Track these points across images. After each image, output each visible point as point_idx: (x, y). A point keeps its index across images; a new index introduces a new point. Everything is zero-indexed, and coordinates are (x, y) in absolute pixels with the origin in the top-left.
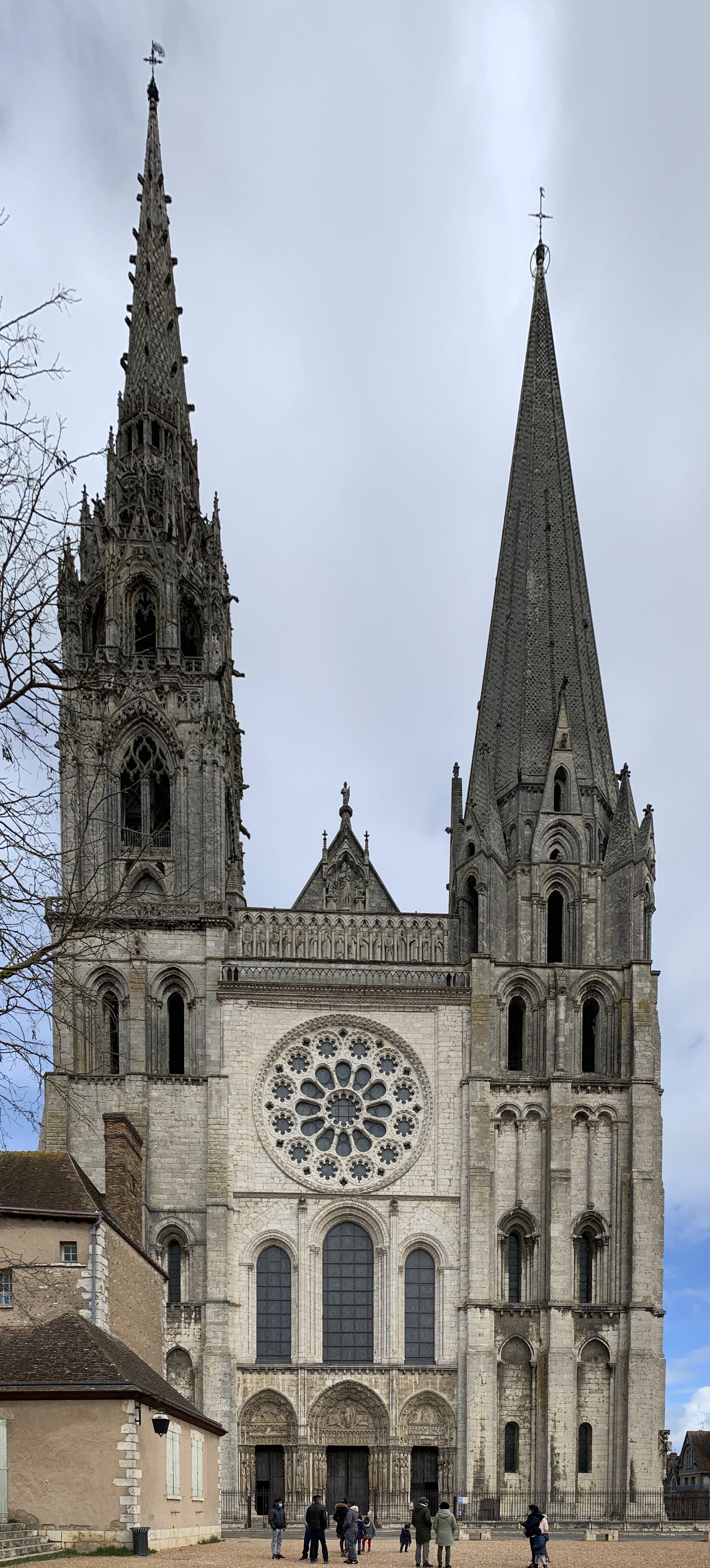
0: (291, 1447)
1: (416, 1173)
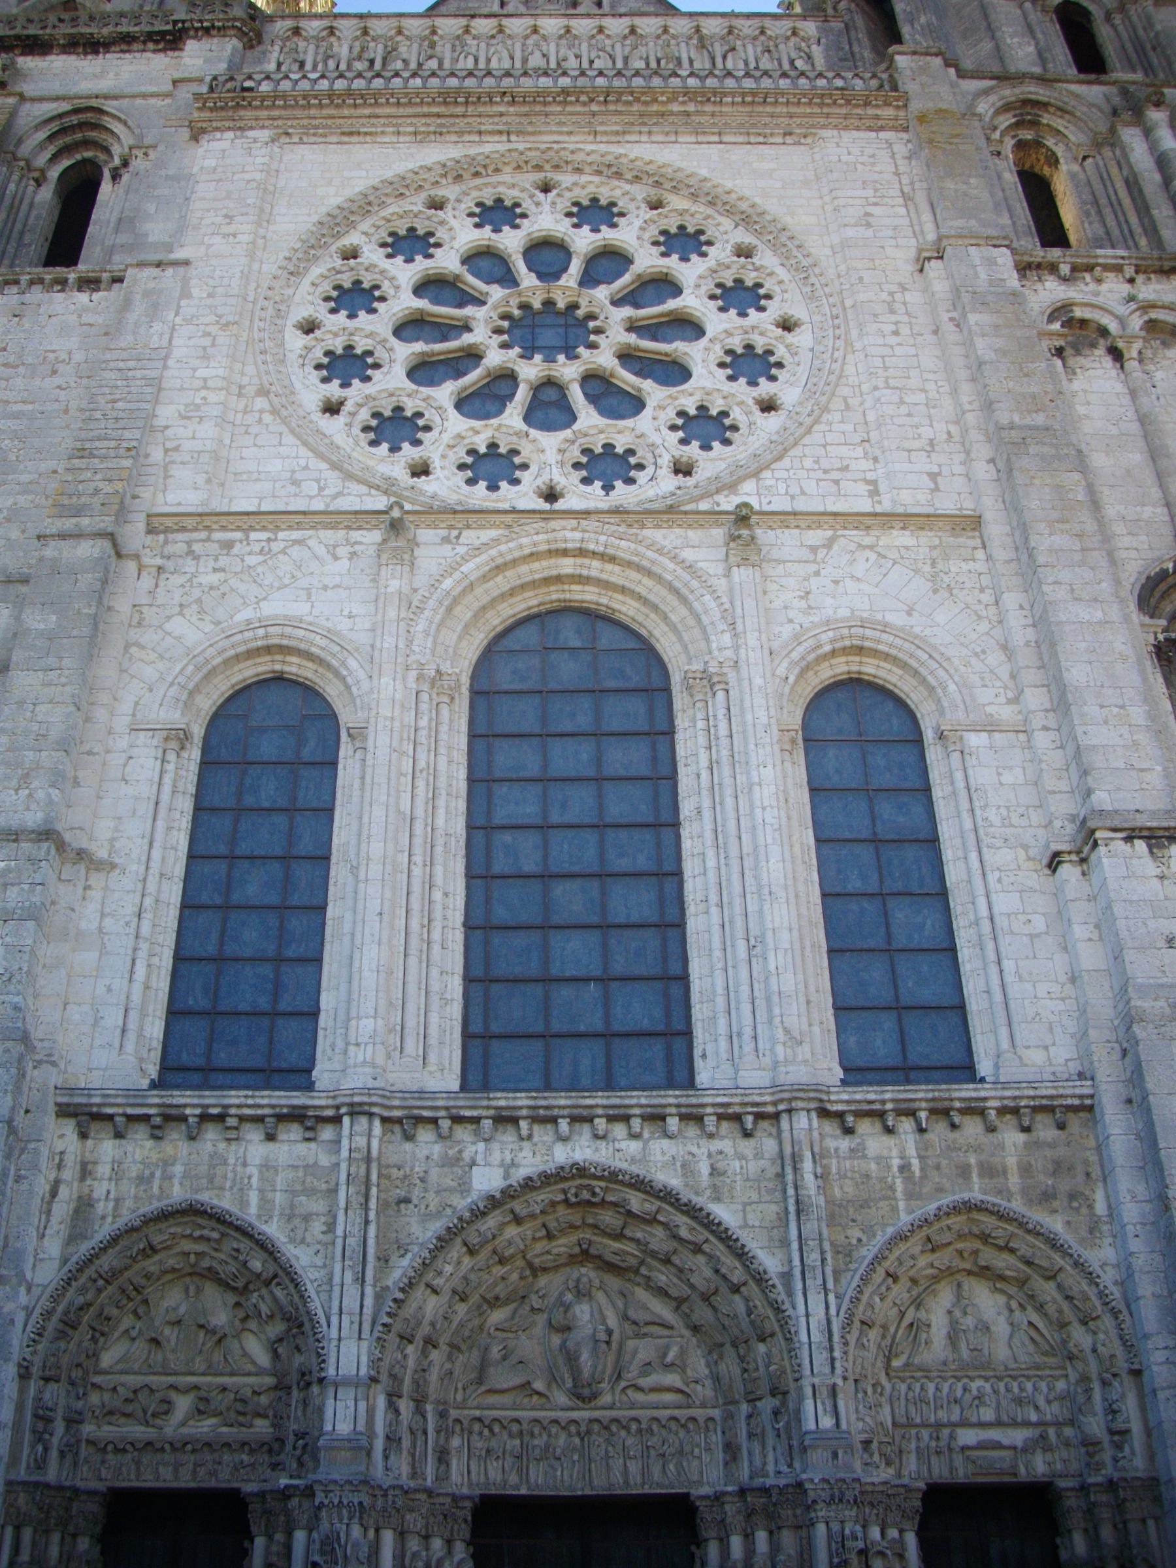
0: (285, 1494)
1: (808, 463)
